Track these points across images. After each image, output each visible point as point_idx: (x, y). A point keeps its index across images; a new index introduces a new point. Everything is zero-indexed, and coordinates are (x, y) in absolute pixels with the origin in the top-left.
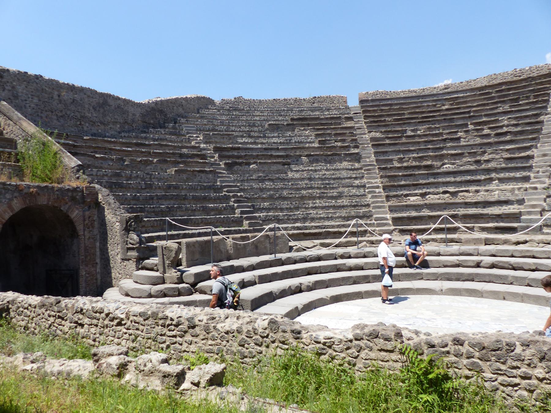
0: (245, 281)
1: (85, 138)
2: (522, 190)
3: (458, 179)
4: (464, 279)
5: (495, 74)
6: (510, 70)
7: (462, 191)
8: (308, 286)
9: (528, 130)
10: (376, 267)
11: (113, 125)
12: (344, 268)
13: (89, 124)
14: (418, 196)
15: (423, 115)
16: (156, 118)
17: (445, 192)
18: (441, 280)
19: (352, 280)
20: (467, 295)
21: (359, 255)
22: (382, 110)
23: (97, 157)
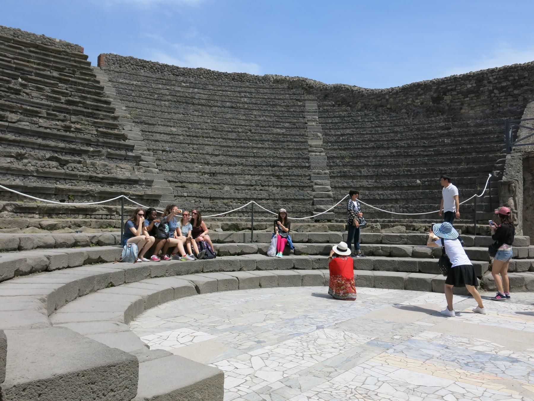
2: (142, 171)
3: (62, 145)
4: (193, 270)
5: (20, 30)
6: (39, 33)
7: (74, 161)
9: (103, 107)
14: (12, 157)
20: (224, 288)
21: (11, 246)
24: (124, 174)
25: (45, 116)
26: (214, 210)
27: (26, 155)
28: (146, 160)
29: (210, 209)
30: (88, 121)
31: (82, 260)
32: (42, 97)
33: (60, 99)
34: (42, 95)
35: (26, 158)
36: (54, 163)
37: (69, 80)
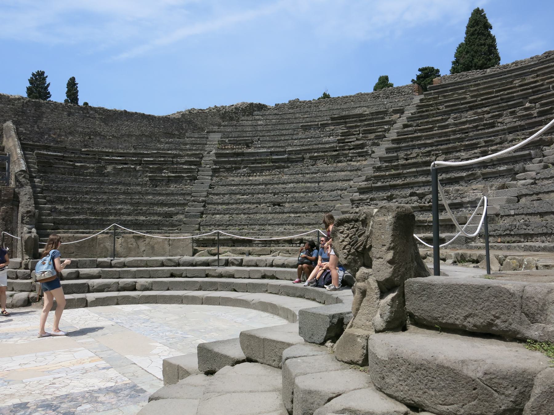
0: (81, 273)
1: (83, 150)
8: (142, 285)
10: (247, 276)
11: (128, 137)
12: (213, 274)
13: (100, 138)
14: (385, 199)
15: (482, 98)
16: (183, 129)
17: (412, 194)
18: (281, 294)
19: (198, 285)
21: (250, 264)
22: (445, 96)
23: (77, 166)
24: (476, 195)
25: (484, 144)
26: (512, 233)
27: (394, 196)
28: (531, 169)
29: (508, 232)
30: (523, 134)
31: (260, 275)
32: (514, 120)
33: (532, 114)
34: (514, 118)
35: (395, 198)
36: (415, 198)
37: (514, 97)
